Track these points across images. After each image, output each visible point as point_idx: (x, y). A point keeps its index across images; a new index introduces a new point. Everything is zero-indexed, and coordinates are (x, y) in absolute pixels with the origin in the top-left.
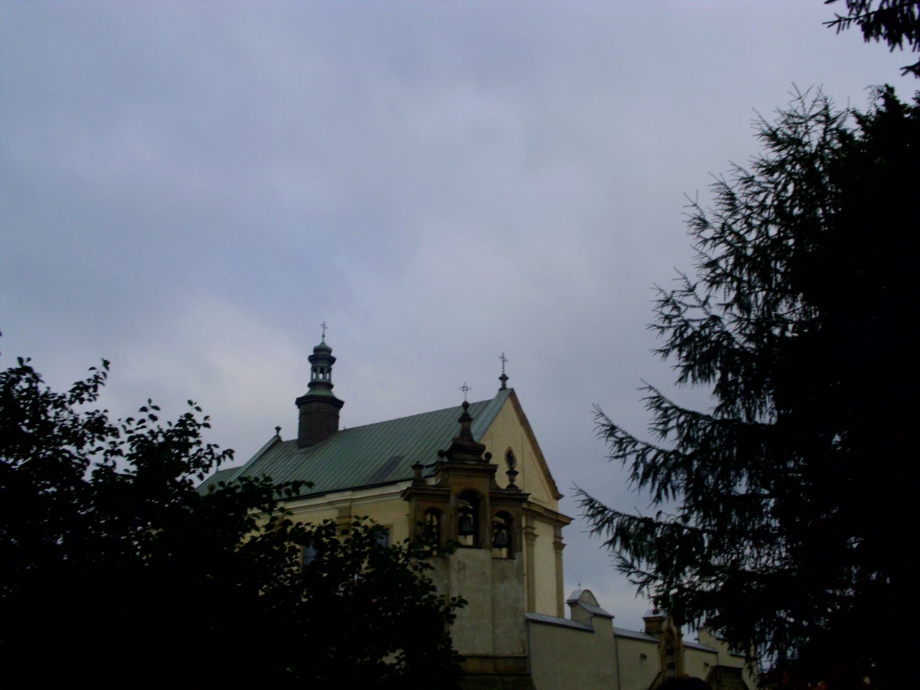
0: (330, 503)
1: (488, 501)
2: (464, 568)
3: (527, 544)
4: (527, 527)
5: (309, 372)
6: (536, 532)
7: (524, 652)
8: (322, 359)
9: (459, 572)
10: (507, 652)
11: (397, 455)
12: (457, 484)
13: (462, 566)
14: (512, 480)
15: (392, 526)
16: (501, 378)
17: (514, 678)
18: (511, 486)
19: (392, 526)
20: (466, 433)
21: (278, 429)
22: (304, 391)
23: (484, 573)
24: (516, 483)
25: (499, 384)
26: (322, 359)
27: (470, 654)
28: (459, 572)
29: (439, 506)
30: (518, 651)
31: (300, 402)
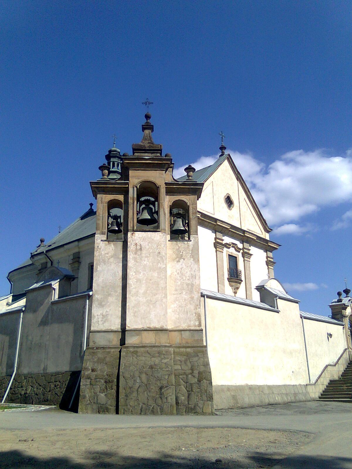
1: (163, 191)
2: (141, 249)
3: (244, 260)
4: (244, 248)
6: (251, 252)
10: (184, 326)
13: (138, 247)
17: (188, 350)
23: (159, 253)
27: (146, 328)
28: (136, 253)
29: (121, 198)
30: (193, 325)
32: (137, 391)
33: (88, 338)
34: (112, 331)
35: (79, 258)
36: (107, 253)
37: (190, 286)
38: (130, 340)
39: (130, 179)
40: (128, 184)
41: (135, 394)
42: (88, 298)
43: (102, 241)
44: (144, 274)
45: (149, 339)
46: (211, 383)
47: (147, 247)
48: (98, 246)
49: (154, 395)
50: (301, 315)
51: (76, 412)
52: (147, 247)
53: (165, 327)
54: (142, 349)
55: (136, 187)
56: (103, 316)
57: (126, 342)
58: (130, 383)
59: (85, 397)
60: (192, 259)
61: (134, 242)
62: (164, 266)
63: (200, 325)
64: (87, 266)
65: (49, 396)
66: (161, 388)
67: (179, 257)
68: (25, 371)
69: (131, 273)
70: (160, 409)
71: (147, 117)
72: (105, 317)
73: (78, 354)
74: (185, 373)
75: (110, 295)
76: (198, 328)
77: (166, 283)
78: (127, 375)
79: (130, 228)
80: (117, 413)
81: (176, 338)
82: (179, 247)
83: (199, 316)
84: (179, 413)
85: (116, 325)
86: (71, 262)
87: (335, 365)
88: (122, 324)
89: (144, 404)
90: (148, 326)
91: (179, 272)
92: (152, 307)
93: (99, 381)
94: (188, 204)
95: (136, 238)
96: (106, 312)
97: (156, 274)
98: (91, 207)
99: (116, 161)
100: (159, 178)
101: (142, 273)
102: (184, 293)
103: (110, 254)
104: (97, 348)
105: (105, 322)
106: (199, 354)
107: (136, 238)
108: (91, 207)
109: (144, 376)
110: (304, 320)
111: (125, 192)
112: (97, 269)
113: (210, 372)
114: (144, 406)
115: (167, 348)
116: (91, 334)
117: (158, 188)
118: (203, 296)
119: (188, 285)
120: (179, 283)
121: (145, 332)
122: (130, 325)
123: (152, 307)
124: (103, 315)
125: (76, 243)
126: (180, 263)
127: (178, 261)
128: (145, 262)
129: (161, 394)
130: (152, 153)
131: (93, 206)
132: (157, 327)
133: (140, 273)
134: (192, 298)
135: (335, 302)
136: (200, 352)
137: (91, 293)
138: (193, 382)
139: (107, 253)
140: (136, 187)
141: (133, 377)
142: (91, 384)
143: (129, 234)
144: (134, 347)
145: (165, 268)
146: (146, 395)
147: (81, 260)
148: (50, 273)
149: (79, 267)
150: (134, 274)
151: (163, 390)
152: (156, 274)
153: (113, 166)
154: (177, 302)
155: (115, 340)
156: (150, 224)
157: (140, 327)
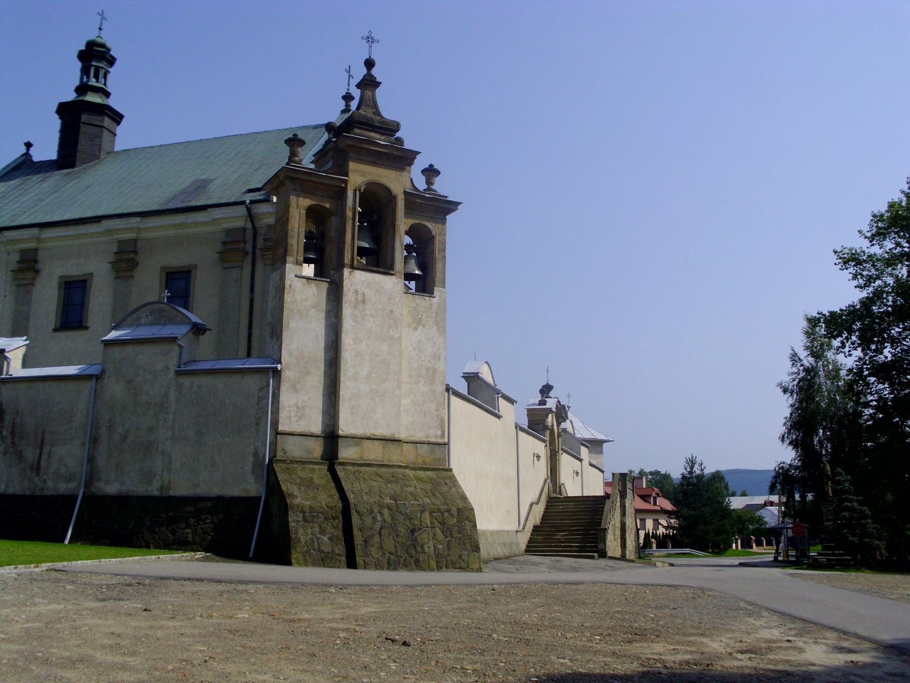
0: (110, 232)
2: (363, 301)
5: (78, 74)
7: (443, 435)
8: (95, 57)
9: (355, 307)
10: (420, 436)
11: (203, 177)
12: (359, 175)
13: (360, 298)
14: (429, 182)
15: (195, 267)
16: (344, 98)
17: (429, 473)
18: (429, 189)
19: (195, 267)
20: (369, 102)
21: (29, 145)
22: (71, 96)
24: (434, 187)
25: (342, 105)
26: (95, 57)
27: (368, 433)
28: (355, 307)
30: (433, 435)
31: (64, 110)
32: (380, 534)
33: (274, 444)
34: (312, 436)
35: (36, 261)
36: (306, 300)
37: (431, 373)
38: (346, 453)
39: (350, 174)
40: (346, 182)
41: (377, 539)
42: (271, 374)
43: (296, 276)
44: (367, 344)
45: (374, 453)
46: (475, 526)
47: (374, 299)
48: (290, 286)
49: (404, 540)
50: (516, 424)
51: (288, 563)
52: (374, 299)
53: (397, 436)
54: (367, 469)
55: (360, 190)
56: (299, 409)
57: (340, 456)
58: (368, 521)
59: (299, 541)
60: (435, 328)
61: (354, 287)
62: (398, 335)
63: (443, 435)
64: (55, 283)
65: (190, 536)
66: (413, 531)
67: (418, 323)
68: (112, 489)
69: (348, 341)
70: (415, 562)
71: (369, 64)
72: (301, 410)
73: (248, 468)
74: (439, 510)
75: (308, 373)
76: (440, 440)
77: (400, 364)
78: (362, 509)
79: (347, 260)
80: (352, 564)
81: (408, 455)
82: (417, 305)
83: (443, 421)
84: (439, 568)
85: (315, 424)
86: (15, 266)
87: (537, 503)
88: (325, 425)
89: (391, 554)
90: (372, 432)
91: (415, 346)
92: (378, 401)
93: (318, 516)
94: (434, 233)
95: (357, 281)
96: (303, 401)
97: (385, 347)
98: (28, 149)
99: (102, 68)
100: (396, 182)
101: (364, 343)
102: (422, 383)
103: (309, 302)
104: (292, 462)
105: (301, 418)
106: (448, 481)
107: (357, 281)
108: (28, 149)
109: (386, 512)
110: (520, 433)
111: (340, 194)
112: (288, 327)
113: (473, 510)
114: (392, 557)
115: (402, 470)
116: (279, 436)
117: (393, 199)
118: (448, 389)
119: (428, 369)
120: (415, 365)
121: (369, 442)
122: (346, 425)
123: (378, 401)
124: (297, 407)
125: (35, 231)
126: (418, 332)
127: (416, 329)
128: (370, 325)
129: (416, 540)
130: (382, 134)
131: (31, 149)
132: (385, 434)
133: (362, 342)
134: (434, 392)
135: (534, 404)
136: (446, 478)
137: (279, 367)
138: (452, 523)
139: (306, 300)
140: (360, 190)
141: (371, 511)
142: (305, 520)
143: (346, 271)
144: (354, 465)
145: (400, 338)
146: (392, 541)
147: (39, 266)
148: (151, 313)
149: (34, 279)
150: (352, 342)
151: (416, 534)
152: (385, 347)
153: (96, 77)
154: (411, 396)
155: (317, 449)
156: (377, 259)
157: (359, 431)
